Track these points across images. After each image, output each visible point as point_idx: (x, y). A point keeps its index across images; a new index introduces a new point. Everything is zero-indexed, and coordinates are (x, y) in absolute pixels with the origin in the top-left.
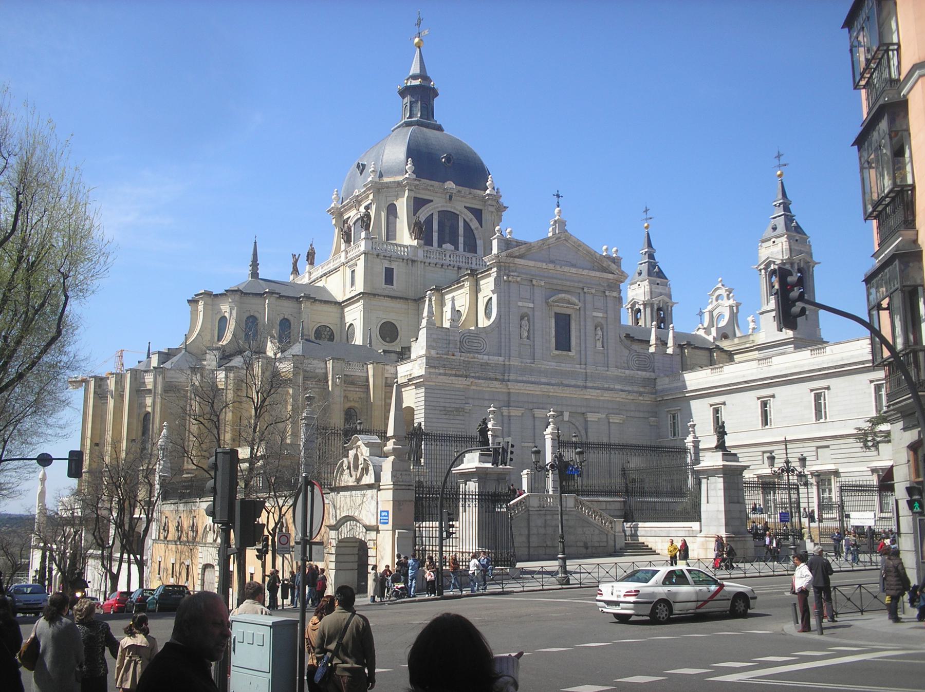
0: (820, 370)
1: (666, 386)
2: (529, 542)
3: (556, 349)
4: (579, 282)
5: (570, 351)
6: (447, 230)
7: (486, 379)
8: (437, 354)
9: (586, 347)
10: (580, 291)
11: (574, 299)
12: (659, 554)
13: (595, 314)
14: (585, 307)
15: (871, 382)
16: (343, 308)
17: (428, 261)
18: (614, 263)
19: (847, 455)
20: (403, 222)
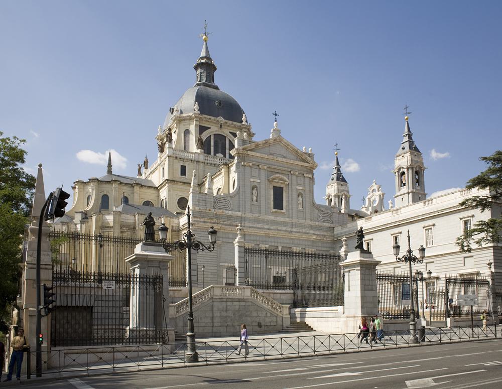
0: (429, 214)
1: (339, 232)
2: (213, 323)
3: (274, 208)
4: (288, 168)
5: (283, 209)
6: (220, 145)
7: (231, 225)
8: (199, 209)
9: (292, 208)
10: (289, 173)
11: (285, 178)
12: (315, 331)
13: (298, 187)
14: (292, 183)
15: (461, 219)
16: (159, 190)
17: (206, 161)
18: (310, 157)
19: (444, 267)
20: (193, 139)
